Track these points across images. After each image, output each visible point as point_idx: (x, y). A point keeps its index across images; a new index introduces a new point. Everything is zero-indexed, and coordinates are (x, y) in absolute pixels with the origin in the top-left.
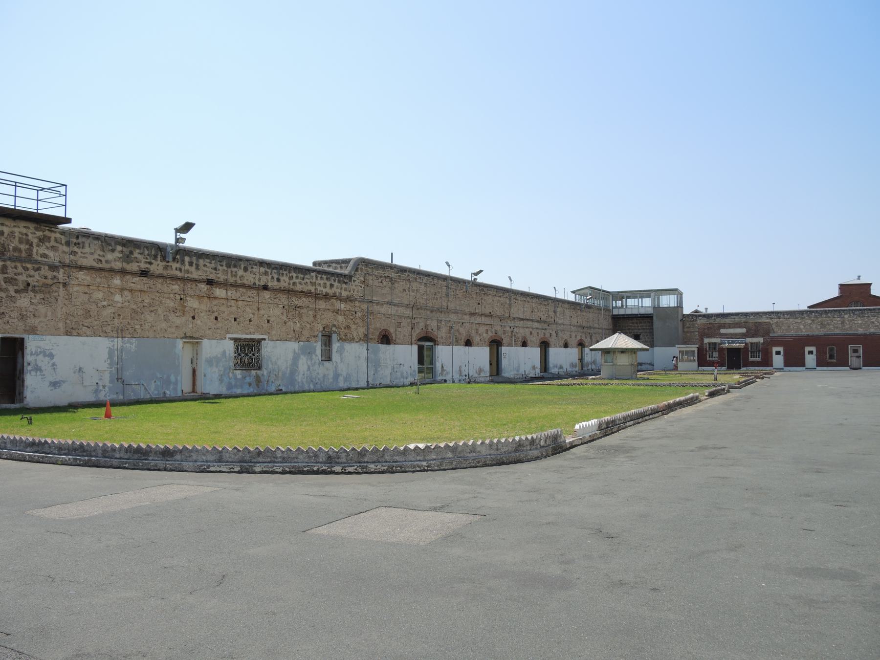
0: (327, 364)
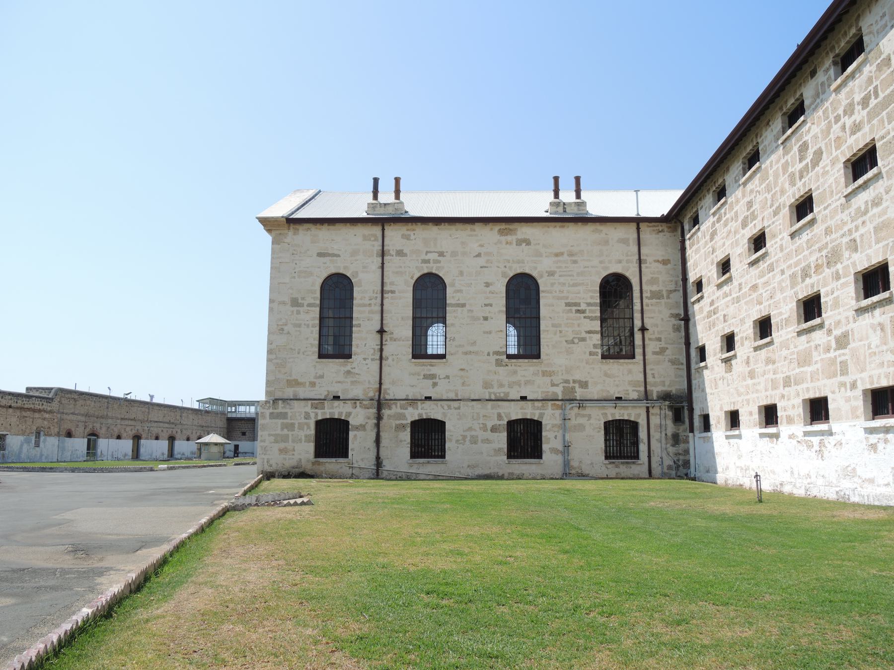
0: (37, 448)
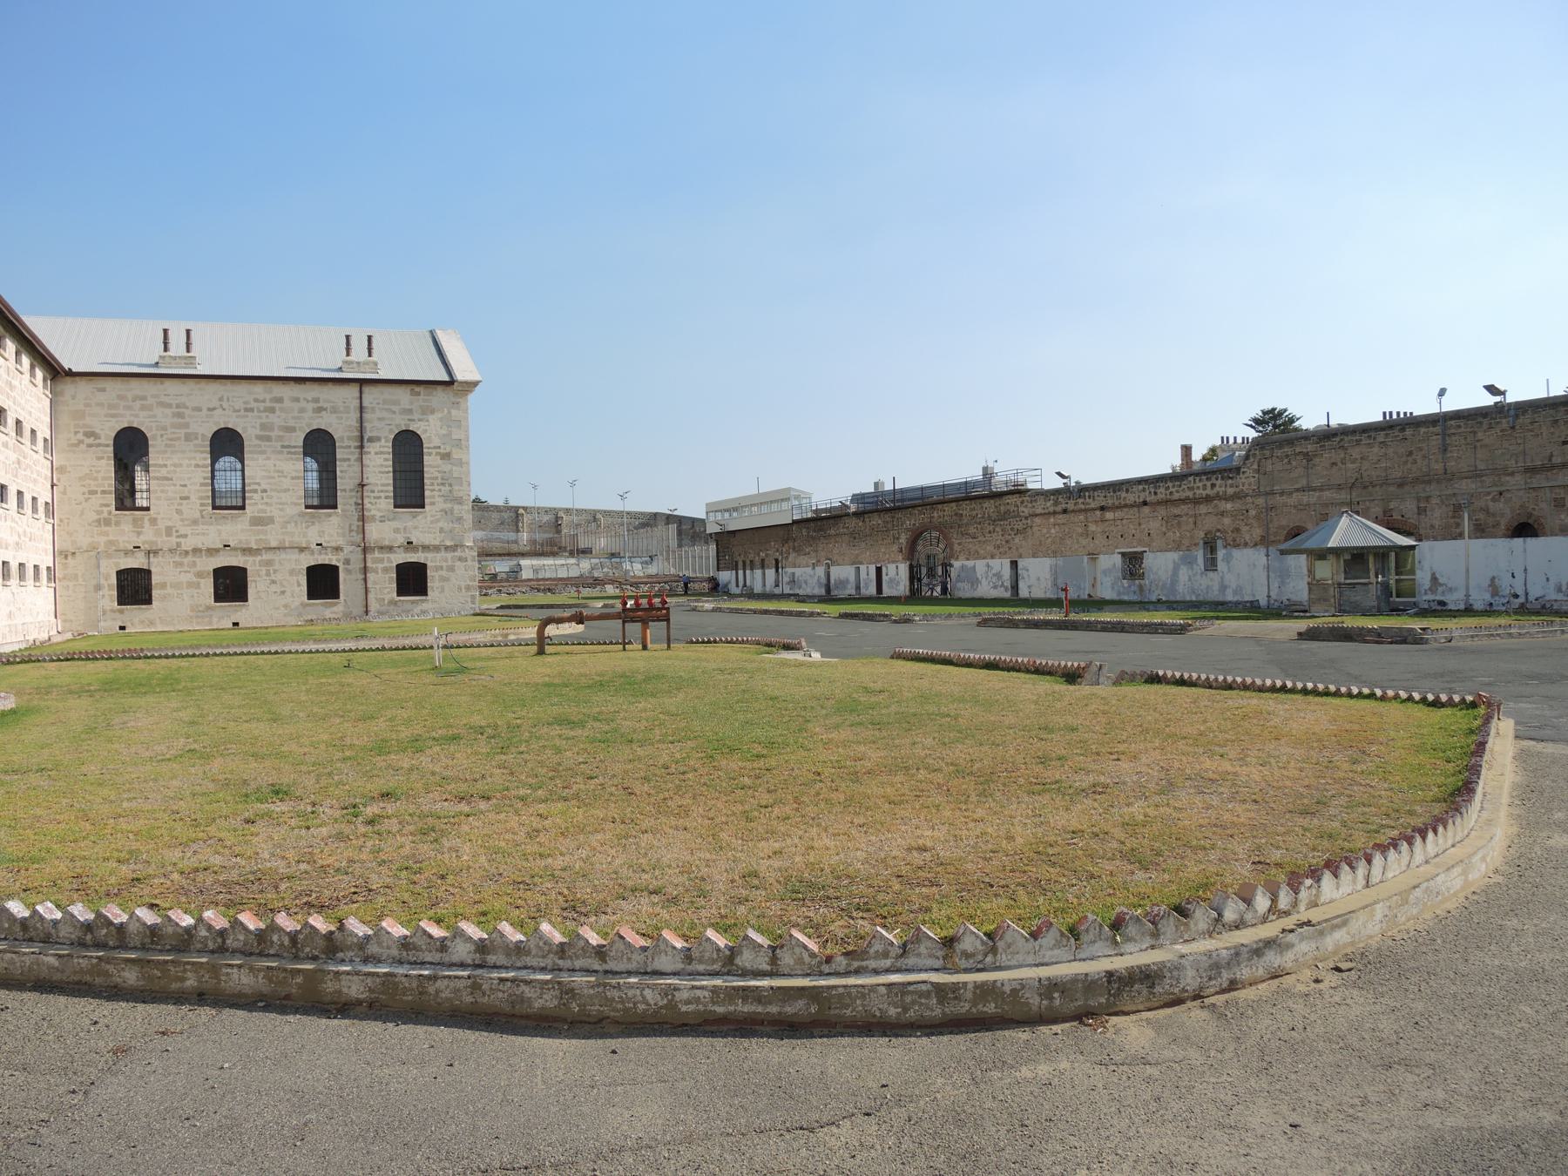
0: (1211, 574)
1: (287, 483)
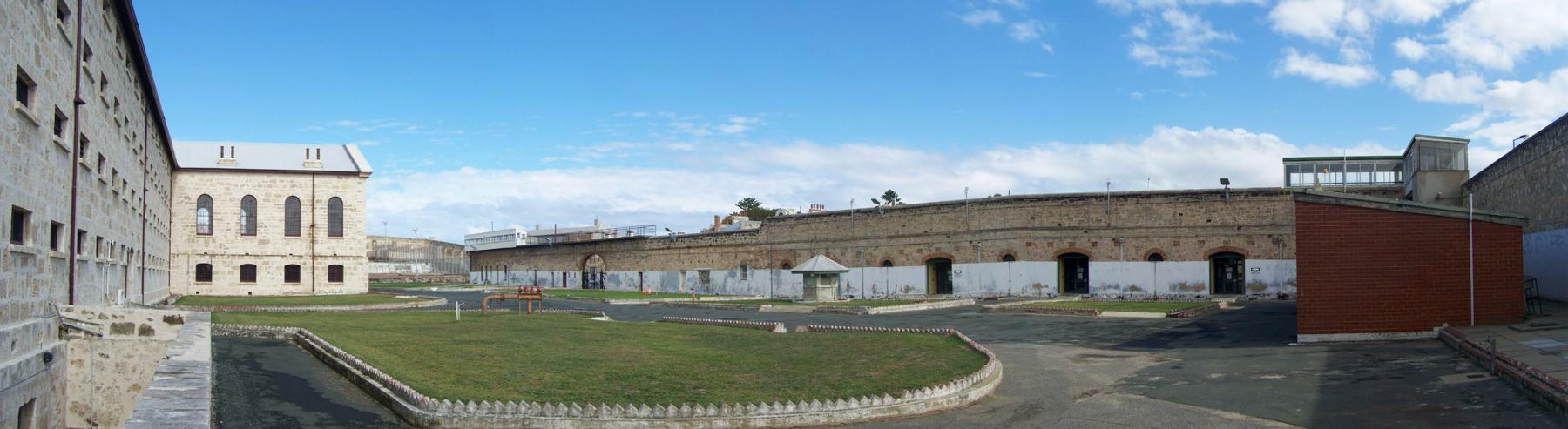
1: (277, 223)
